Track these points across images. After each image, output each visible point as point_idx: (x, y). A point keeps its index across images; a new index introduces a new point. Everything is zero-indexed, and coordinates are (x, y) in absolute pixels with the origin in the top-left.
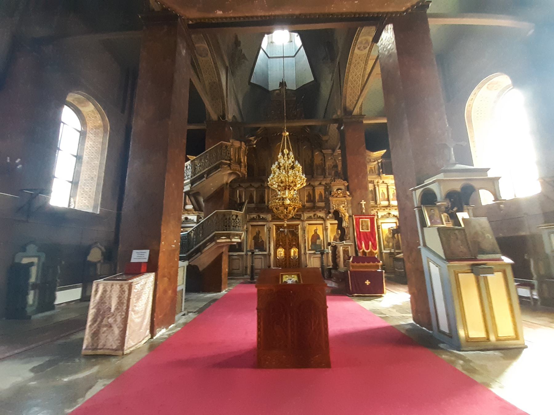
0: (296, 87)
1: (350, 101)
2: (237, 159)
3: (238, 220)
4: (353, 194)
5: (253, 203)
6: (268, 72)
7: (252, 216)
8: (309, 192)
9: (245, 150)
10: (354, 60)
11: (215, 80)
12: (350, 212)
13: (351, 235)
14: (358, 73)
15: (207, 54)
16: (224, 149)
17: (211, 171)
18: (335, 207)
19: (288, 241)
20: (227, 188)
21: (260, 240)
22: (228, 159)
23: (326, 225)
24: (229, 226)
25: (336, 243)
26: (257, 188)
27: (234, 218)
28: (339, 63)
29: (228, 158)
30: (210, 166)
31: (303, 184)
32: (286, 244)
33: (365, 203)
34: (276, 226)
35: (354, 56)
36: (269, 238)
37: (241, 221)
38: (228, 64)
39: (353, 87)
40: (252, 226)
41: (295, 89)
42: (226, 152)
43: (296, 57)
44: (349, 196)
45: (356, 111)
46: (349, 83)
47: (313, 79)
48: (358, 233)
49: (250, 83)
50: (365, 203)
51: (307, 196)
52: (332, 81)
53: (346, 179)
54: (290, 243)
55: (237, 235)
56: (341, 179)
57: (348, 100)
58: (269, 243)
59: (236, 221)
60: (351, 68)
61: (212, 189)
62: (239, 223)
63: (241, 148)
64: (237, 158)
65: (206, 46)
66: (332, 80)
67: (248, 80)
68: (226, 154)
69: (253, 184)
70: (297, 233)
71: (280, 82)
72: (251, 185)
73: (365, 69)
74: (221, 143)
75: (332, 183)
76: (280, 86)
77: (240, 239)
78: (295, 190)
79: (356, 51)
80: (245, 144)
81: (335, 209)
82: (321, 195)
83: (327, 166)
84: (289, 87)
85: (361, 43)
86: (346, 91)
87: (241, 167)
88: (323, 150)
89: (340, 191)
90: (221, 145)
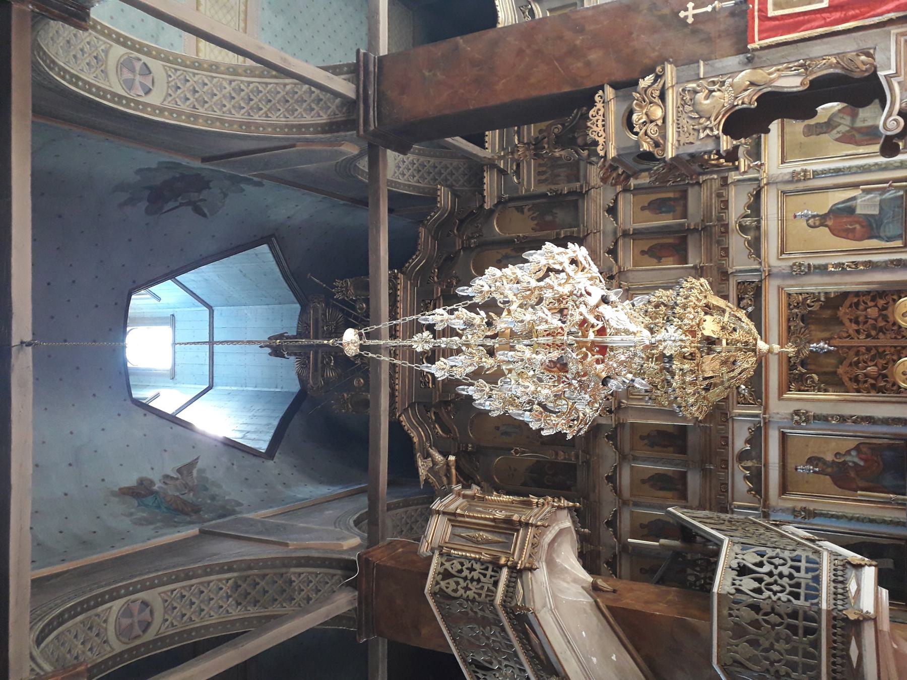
0: (295, 303)
1: (313, 109)
2: (496, 538)
3: (761, 565)
4: (646, 61)
5: (683, 475)
6: (247, 391)
7: (742, 485)
8: (643, 253)
9: (465, 496)
10: (185, 107)
11: (230, 582)
12: (733, 61)
13: (848, 46)
14: (224, 91)
15: (145, 604)
16: (453, 585)
17: (537, 657)
18: (708, 131)
19: (862, 337)
20: (614, 591)
21: (853, 458)
22: (491, 577)
23: (787, 177)
24: (794, 615)
25: (890, 115)
26: (623, 457)
27: (756, 585)
28: (205, 160)
29: (489, 573)
30: (515, 654)
31: (574, 262)
33: (690, 5)
35: (171, 106)
36: (843, 419)
37: (770, 552)
38: (193, 531)
39: (270, 105)
40: (784, 489)
41: (297, 306)
42: (465, 579)
43: (211, 304)
44: (658, 77)
45: (343, 86)
46: (257, 118)
47: (264, 248)
48: (837, 15)
49: (270, 453)
50: (690, 5)
51: (659, 262)
52: (265, 182)
53: (586, 99)
54: (873, 333)
55: (839, 581)
56: (586, 118)
57: (308, 119)
58: (870, 420)
59: (767, 579)
60: (211, 114)
61: (614, 658)
62: (777, 561)
63: (454, 514)
64: (490, 536)
65: (117, 605)
66: (260, 184)
67: (256, 461)
68: (472, 580)
69: (606, 470)
70: (822, 299)
71: (270, 354)
72: (611, 479)
73: (214, 67)
74: (434, 594)
75: (602, 153)
76: (283, 356)
77: (858, 567)
78: (605, 300)
79: (155, 98)
80: (445, 494)
81: (716, 132)
82: (658, 207)
83: (543, 189)
84: (290, 326)
85: (129, 84)
86: (282, 127)
87: (527, 525)
88: (487, 206)
89: (635, 117)
90: (441, 596)
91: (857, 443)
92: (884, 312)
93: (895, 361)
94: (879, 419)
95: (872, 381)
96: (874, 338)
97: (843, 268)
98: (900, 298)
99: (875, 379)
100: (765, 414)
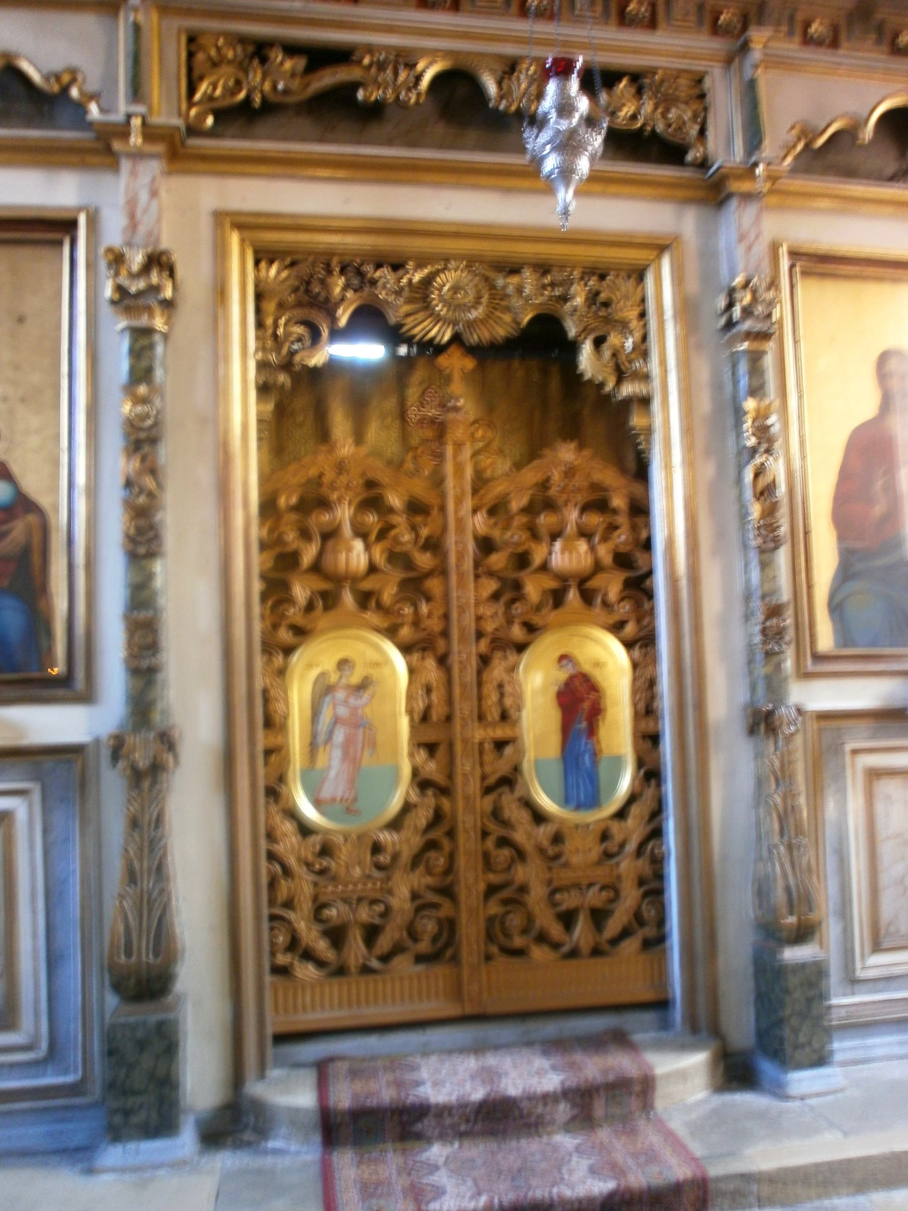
19: (480, 523)
32: (442, 571)
34: (264, 256)
70: (628, 389)
91: (44, 501)
92: (573, 595)
93: (391, 633)
94: (149, 577)
95: (309, 554)
96: (477, 565)
97: (754, 451)
98: (629, 645)
99: (316, 568)
100: (150, 133)
